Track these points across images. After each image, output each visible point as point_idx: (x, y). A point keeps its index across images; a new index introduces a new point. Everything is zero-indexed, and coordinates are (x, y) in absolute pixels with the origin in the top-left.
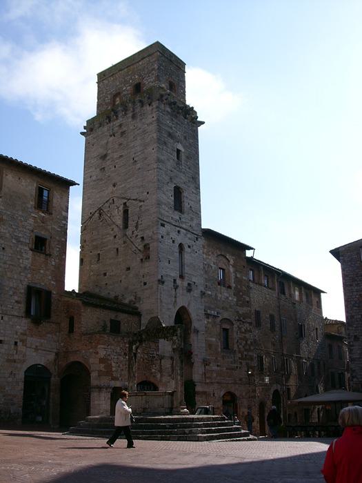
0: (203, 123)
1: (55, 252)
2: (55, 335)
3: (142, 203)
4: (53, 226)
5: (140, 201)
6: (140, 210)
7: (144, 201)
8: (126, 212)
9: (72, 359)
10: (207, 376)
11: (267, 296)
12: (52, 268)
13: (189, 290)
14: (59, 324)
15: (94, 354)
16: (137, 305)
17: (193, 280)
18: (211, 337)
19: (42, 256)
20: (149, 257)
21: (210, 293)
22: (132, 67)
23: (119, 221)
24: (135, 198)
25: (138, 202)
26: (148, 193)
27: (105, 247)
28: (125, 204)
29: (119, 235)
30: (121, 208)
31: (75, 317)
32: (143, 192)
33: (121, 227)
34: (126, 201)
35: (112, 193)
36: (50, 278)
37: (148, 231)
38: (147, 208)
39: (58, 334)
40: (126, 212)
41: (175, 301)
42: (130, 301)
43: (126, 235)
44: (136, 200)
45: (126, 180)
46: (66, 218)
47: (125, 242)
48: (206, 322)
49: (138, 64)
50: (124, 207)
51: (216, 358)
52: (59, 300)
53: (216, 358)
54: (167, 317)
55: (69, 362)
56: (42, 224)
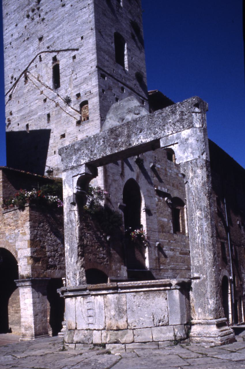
3: (75, 53)
5: (73, 50)
7: (77, 50)
18: (162, 217)
20: (88, 118)
21: (159, 166)
24: (66, 48)
25: (70, 52)
26: (82, 38)
27: (34, 115)
28: (55, 59)
32: (75, 39)
33: (51, 87)
34: (54, 54)
35: (39, 48)
37: (85, 86)
38: (81, 57)
50: (53, 63)
51: (169, 241)
53: (169, 241)
54: (115, 190)
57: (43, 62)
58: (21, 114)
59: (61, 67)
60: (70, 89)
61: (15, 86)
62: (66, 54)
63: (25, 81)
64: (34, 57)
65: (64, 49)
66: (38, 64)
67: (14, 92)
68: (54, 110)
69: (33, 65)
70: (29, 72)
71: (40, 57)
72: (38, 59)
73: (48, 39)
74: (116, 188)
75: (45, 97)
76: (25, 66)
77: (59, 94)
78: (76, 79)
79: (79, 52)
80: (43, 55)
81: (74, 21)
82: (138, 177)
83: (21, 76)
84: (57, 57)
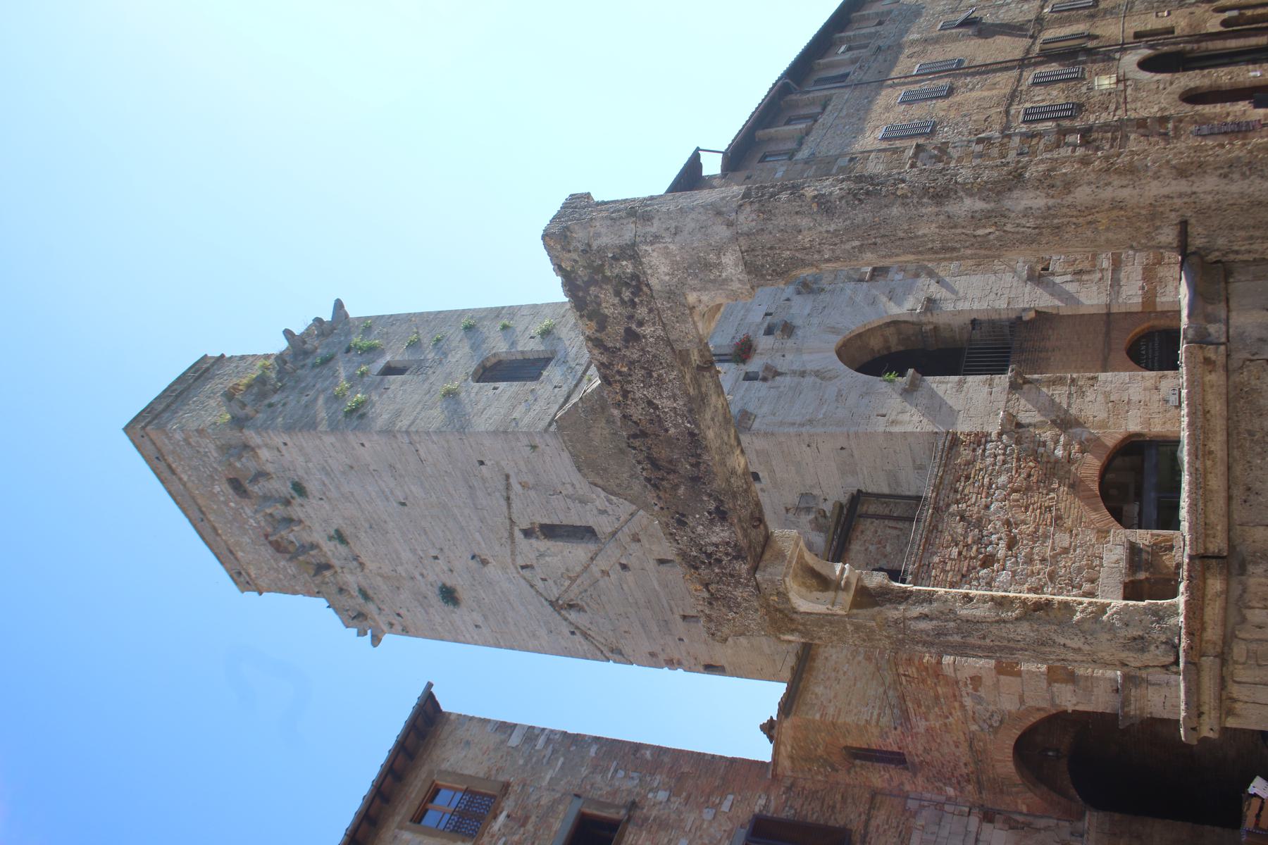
0: (339, 305)
1: (626, 783)
2: (914, 814)
3: (513, 481)
4: (545, 783)
5: (508, 487)
6: (533, 488)
7: (507, 477)
8: (551, 531)
9: (1005, 765)
10: (1086, 265)
11: (844, 112)
12: (676, 803)
13: (788, 329)
14: (874, 794)
15: (982, 692)
16: (828, 507)
17: (759, 319)
19: (631, 828)
22: (200, 501)
23: (577, 553)
24: (503, 503)
25: (513, 496)
26: (482, 463)
28: (528, 533)
29: (610, 557)
30: (543, 544)
31: (842, 742)
32: (484, 480)
33: (592, 547)
36: (708, 814)
39: (912, 804)
40: (551, 531)
41: (817, 374)
42: (819, 527)
43: (614, 534)
44: (508, 498)
45: (462, 528)
46: (531, 734)
47: (636, 539)
48: (899, 276)
49: (189, 485)
52: (789, 789)
55: (1017, 778)
56: (530, 827)
57: (534, 563)
58: (655, 629)
59: (546, 521)
60: (597, 503)
61: (589, 635)
62: (516, 504)
63: (579, 611)
64: (522, 581)
65: (505, 509)
66: (540, 571)
67: (603, 641)
68: (647, 546)
69: (540, 585)
70: (557, 600)
71: (523, 567)
72: (526, 573)
73: (483, 545)
74: (862, 396)
75: (619, 568)
76: (543, 606)
77: (610, 530)
78: (573, 485)
79: (512, 474)
80: (520, 562)
81: (446, 478)
82: (834, 330)
83: (566, 619)
84: (525, 527)
